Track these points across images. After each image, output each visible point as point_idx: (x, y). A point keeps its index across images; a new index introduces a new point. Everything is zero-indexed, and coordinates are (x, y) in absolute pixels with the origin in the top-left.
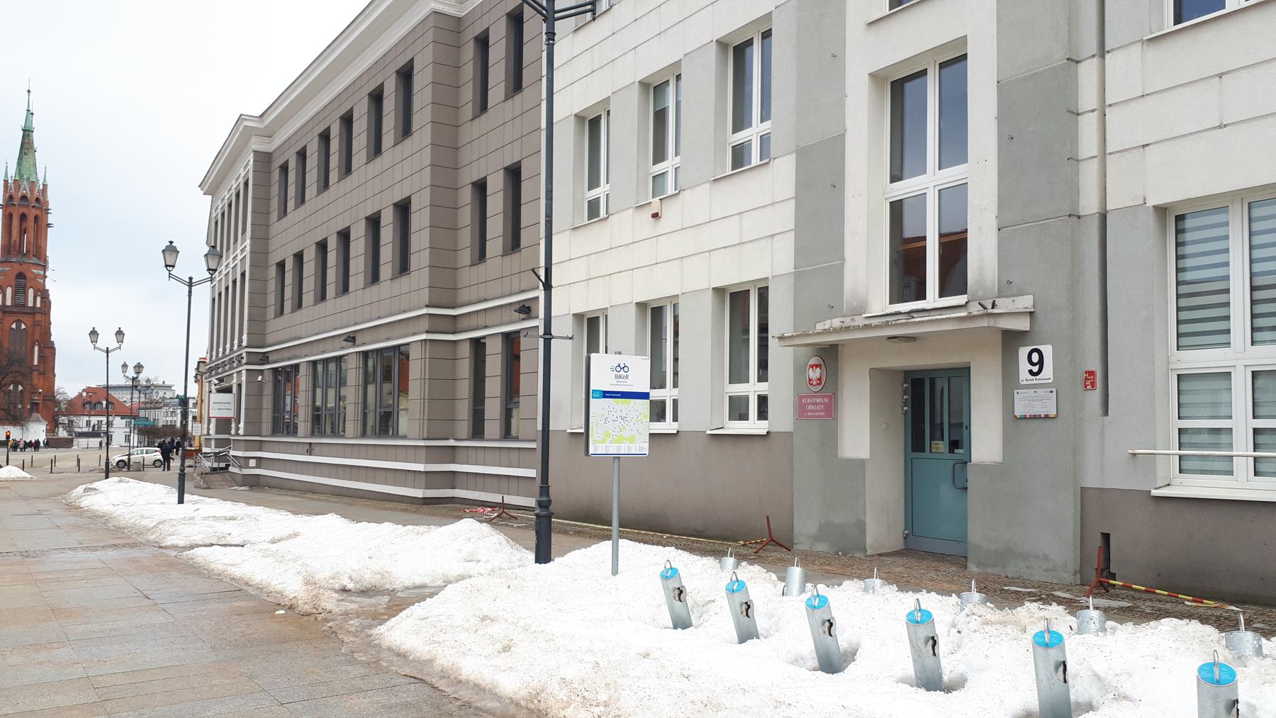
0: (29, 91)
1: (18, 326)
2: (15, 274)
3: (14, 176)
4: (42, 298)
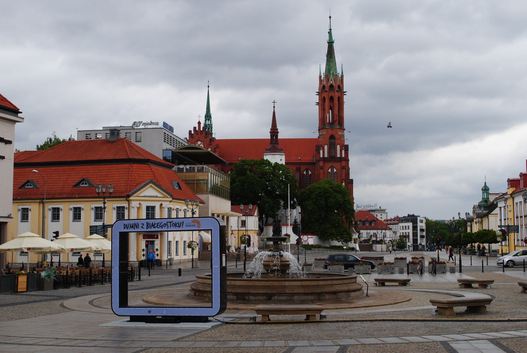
0: (330, 17)
1: (332, 170)
2: (329, 136)
3: (324, 73)
4: (345, 151)
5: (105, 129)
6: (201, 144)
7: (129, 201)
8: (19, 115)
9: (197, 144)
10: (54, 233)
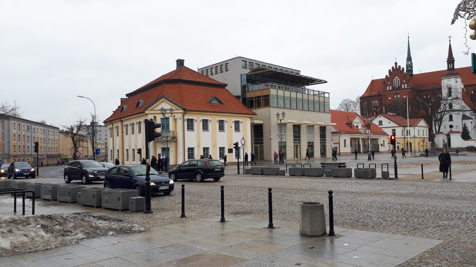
6: (398, 78)
9: (395, 78)
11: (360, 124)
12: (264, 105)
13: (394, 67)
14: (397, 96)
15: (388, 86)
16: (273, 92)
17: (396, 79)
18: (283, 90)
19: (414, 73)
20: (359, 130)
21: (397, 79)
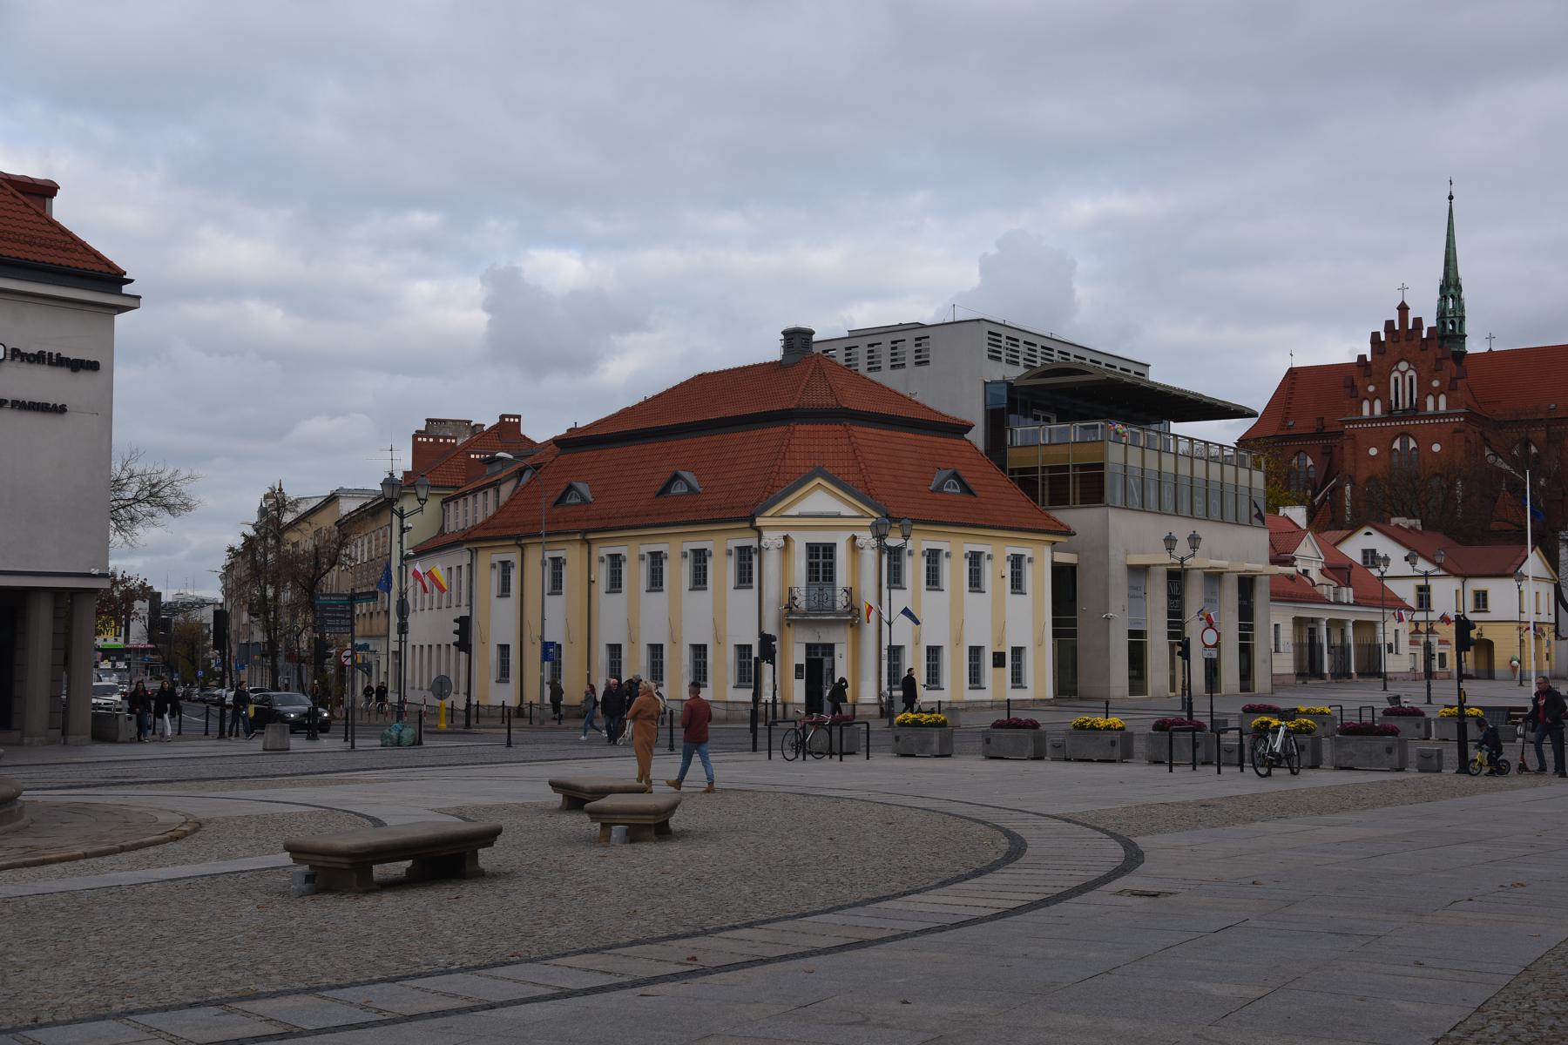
5: (854, 334)
6: (1409, 368)
7: (759, 530)
8: (126, 289)
9: (1397, 370)
10: (456, 621)
11: (1314, 564)
12: (1078, 501)
13: (1393, 321)
14: (1404, 445)
15: (1365, 398)
16: (1115, 454)
17: (1403, 374)
18: (1141, 444)
19: (1475, 345)
20: (1318, 589)
21: (1405, 372)
